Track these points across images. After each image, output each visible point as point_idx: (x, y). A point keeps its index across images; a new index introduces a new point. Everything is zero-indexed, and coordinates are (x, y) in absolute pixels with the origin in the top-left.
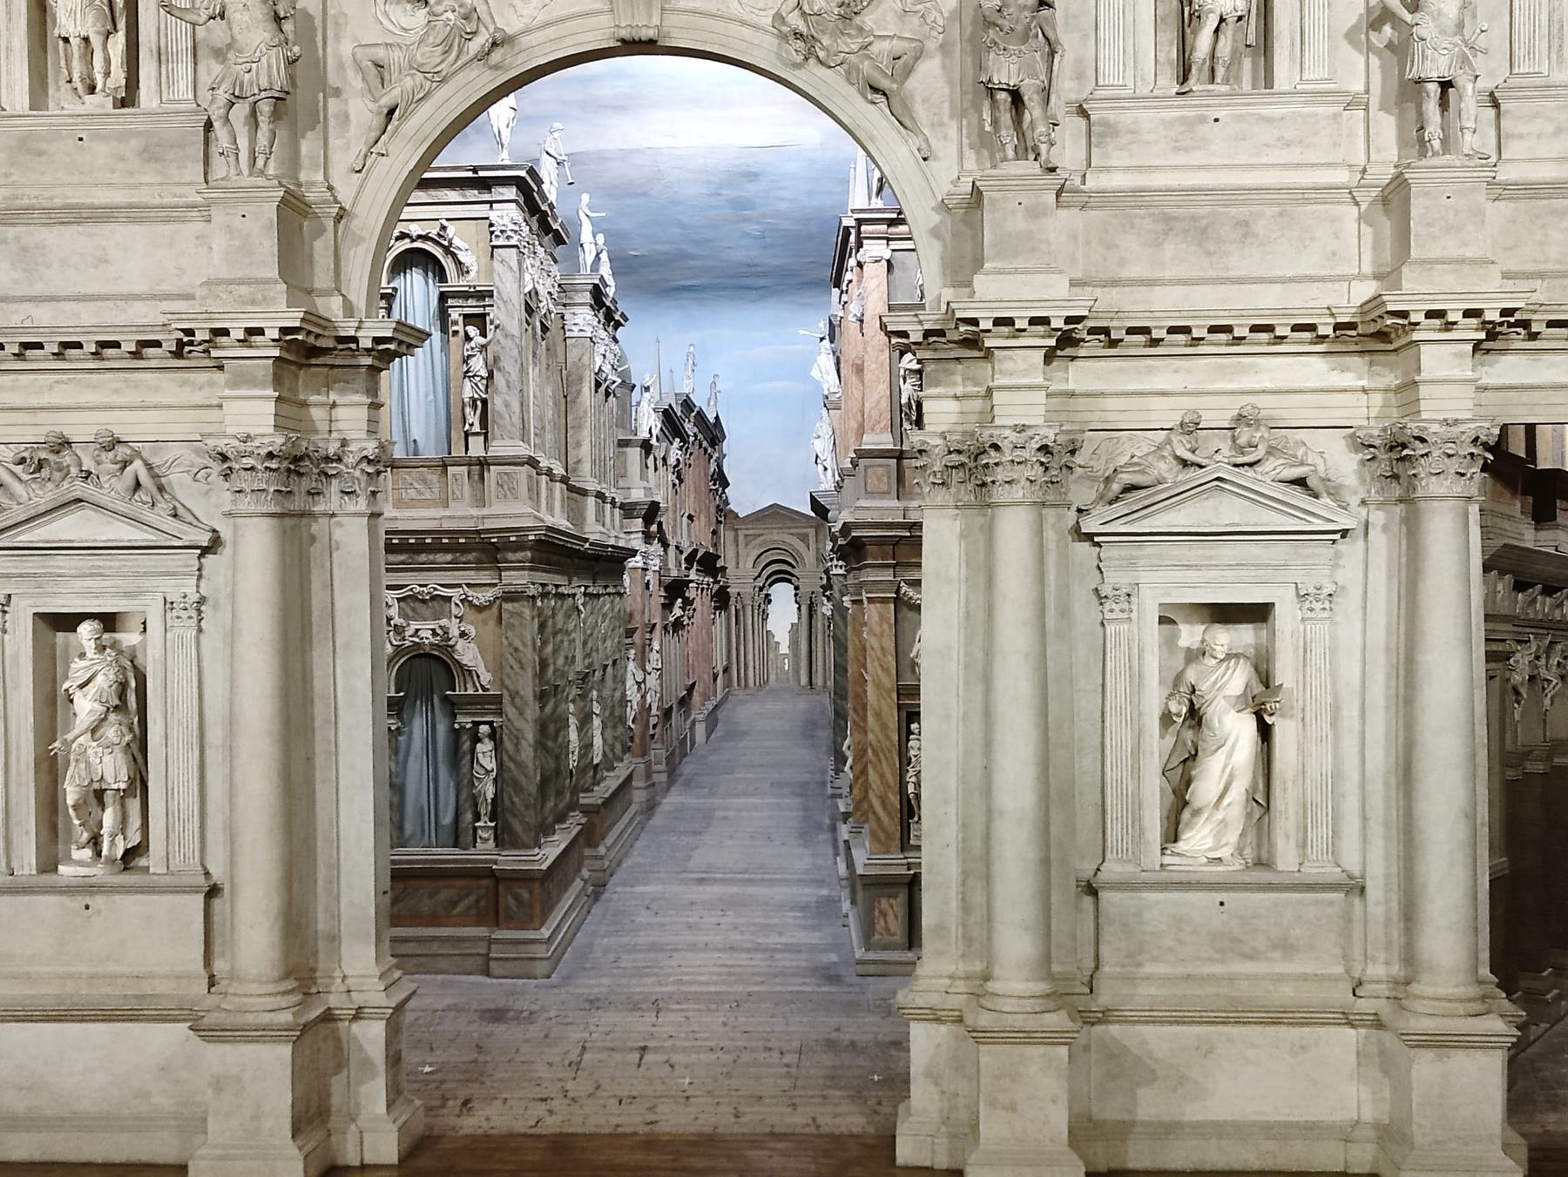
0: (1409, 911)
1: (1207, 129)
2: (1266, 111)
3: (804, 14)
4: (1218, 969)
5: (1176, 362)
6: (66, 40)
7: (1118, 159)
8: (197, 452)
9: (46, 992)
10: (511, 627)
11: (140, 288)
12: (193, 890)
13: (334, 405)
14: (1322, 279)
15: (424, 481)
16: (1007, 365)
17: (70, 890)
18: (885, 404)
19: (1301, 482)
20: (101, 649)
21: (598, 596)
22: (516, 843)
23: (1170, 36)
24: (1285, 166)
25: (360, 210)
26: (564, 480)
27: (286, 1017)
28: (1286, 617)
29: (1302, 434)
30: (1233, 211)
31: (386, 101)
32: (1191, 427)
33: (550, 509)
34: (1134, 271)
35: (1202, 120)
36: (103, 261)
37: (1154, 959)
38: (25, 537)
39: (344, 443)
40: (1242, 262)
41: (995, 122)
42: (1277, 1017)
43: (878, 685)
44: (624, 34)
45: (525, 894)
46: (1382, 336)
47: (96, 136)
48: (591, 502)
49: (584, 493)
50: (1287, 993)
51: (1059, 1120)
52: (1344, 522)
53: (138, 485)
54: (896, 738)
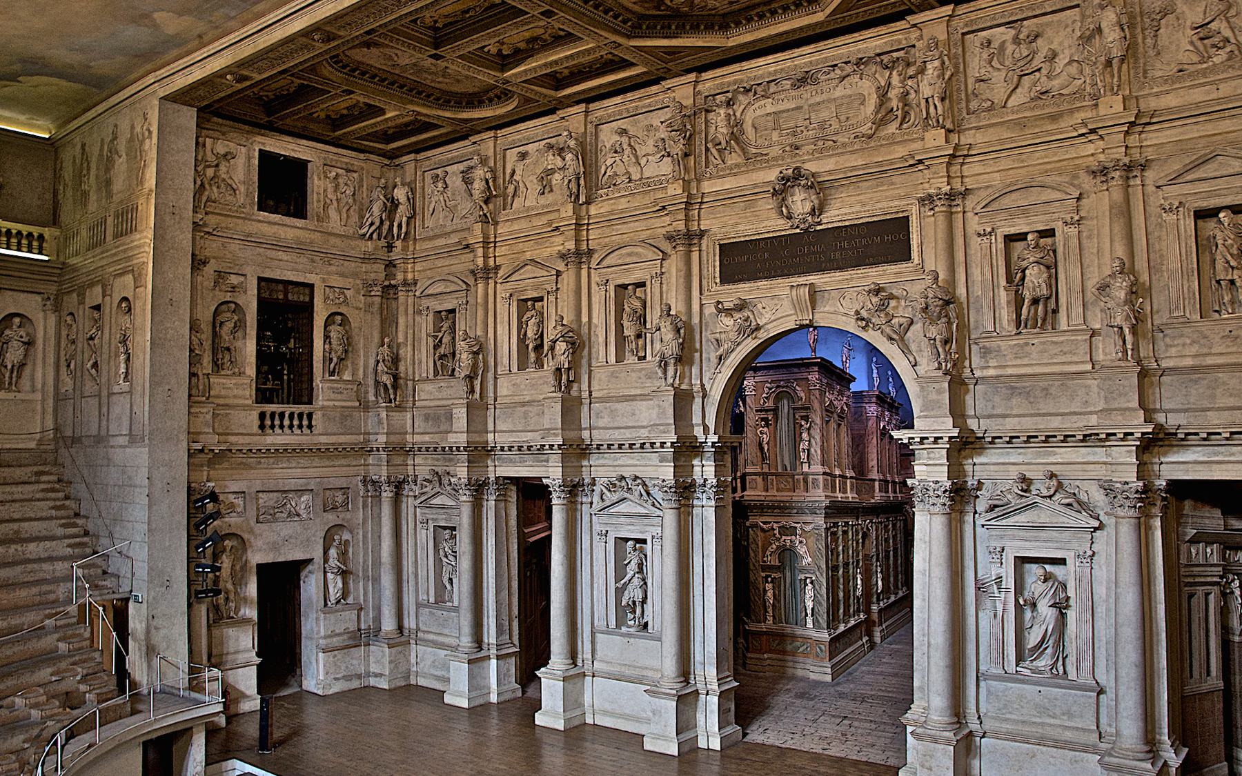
1: (1027, 349)
2: (1054, 339)
4: (1038, 720)
5: (1022, 450)
7: (992, 363)
10: (817, 540)
13: (703, 466)
14: (1080, 414)
15: (787, 481)
16: (932, 455)
17: (622, 635)
20: (635, 550)
21: (881, 523)
22: (820, 628)
24: (1063, 363)
25: (713, 393)
26: (851, 478)
27: (675, 692)
29: (1077, 483)
30: (1041, 384)
33: (844, 491)
34: (999, 411)
35: (1027, 344)
36: (634, 414)
37: (1010, 713)
39: (705, 480)
40: (1045, 407)
42: (1063, 745)
45: (823, 647)
47: (633, 370)
48: (877, 484)
49: (874, 480)
50: (1068, 735)
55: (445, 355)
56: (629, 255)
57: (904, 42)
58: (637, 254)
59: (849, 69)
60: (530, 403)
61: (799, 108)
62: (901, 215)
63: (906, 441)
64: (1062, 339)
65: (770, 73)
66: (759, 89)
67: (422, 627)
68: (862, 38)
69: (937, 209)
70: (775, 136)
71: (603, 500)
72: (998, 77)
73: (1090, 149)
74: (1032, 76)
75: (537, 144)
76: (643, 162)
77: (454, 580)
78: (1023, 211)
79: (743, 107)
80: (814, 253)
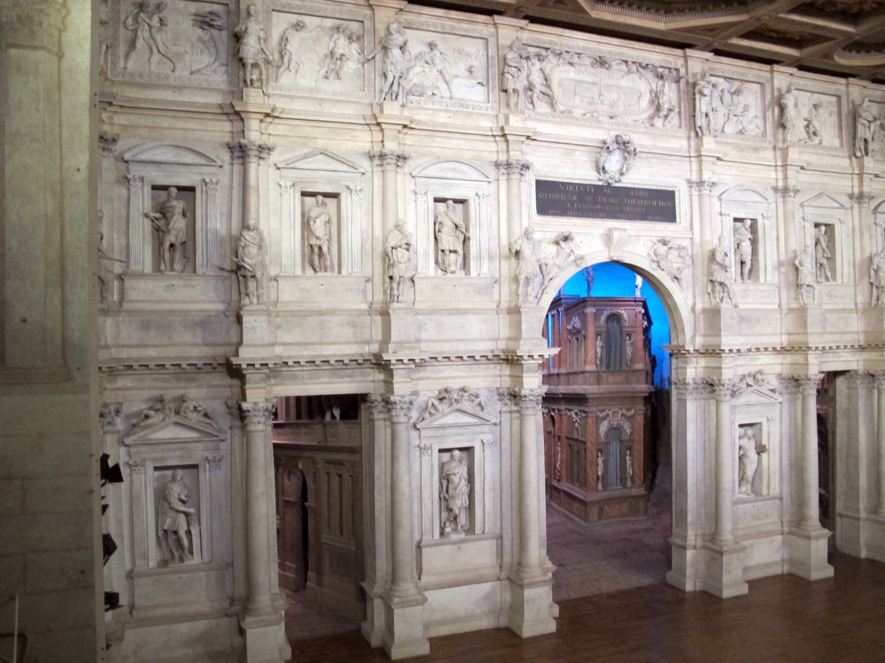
0: (800, 503)
3: (656, 255)
6: (443, 251)
8: (490, 391)
9: (447, 578)
11: (476, 336)
12: (493, 538)
18: (594, 357)
19: (772, 390)
23: (739, 266)
24: (765, 303)
28: (765, 427)
31: (550, 276)
32: (750, 375)
38: (436, 423)
41: (713, 291)
43: (592, 443)
44: (615, 258)
46: (788, 351)
50: (768, 528)
51: (740, 572)
52: (780, 400)
53: (480, 404)
54: (595, 458)
55: (172, 245)
56: (453, 170)
57: (673, 64)
58: (461, 172)
59: (634, 68)
60: (332, 312)
61: (594, 84)
62: (670, 189)
63: (691, 351)
64: (763, 288)
65: (579, 48)
66: (567, 56)
67: (138, 602)
68: (652, 50)
69: (705, 192)
70: (577, 100)
71: (431, 414)
72: (722, 111)
73: (773, 175)
74: (737, 118)
75: (319, 19)
76: (456, 82)
77: (195, 531)
78: (744, 204)
79: (550, 66)
80: (611, 204)
